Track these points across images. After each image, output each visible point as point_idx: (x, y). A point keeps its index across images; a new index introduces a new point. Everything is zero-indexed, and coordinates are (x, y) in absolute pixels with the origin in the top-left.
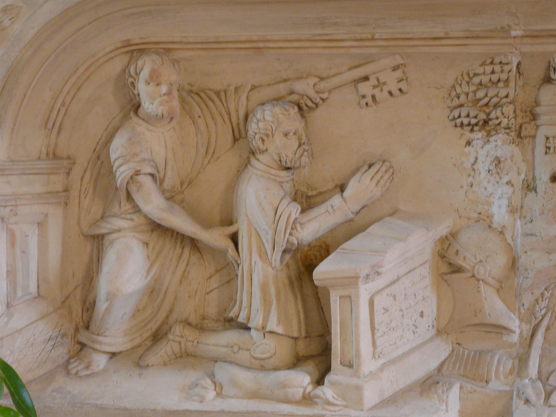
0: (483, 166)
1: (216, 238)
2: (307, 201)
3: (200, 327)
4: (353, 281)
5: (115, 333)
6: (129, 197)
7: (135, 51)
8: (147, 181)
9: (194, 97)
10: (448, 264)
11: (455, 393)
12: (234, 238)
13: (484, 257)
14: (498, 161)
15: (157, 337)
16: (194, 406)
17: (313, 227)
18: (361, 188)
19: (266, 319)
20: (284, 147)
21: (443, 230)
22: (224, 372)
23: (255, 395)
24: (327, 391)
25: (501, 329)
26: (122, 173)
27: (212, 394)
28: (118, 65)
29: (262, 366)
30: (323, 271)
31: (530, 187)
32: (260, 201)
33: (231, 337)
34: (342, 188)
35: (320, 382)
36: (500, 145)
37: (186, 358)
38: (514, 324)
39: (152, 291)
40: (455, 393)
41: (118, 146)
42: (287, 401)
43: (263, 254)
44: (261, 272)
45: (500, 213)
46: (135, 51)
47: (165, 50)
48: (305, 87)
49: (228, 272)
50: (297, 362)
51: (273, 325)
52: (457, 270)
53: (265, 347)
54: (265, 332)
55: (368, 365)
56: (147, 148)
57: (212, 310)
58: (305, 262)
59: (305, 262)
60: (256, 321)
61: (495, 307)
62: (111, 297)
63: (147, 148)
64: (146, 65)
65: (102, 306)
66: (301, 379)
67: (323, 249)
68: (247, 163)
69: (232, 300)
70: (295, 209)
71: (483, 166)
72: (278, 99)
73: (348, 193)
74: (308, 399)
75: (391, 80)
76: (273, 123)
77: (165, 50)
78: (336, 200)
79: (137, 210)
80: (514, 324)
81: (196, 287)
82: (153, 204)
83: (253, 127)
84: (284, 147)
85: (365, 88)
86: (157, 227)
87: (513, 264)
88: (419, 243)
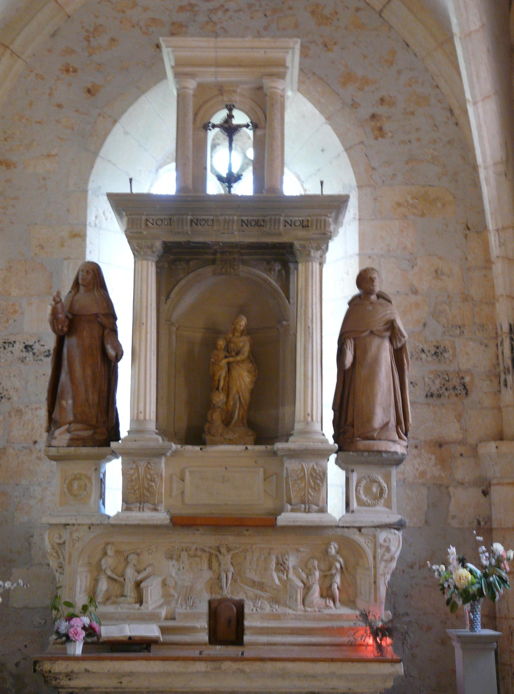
0: (171, 566)
1: (121, 579)
2: (139, 572)
3: (117, 597)
4: (147, 587)
5: (100, 599)
6: (104, 571)
7: (107, 544)
8: (108, 569)
9: (118, 552)
10: (164, 584)
11: (165, 607)
12: (125, 580)
13: (171, 582)
14: (173, 565)
15: (108, 599)
16: (116, 611)
17: (140, 577)
18: (149, 570)
19: (131, 594)
20: (135, 562)
21: (163, 577)
22: (122, 605)
23: (129, 609)
24: (142, 607)
25: (173, 596)
26: (104, 567)
27: (120, 609)
28: (102, 546)
29: (129, 604)
30: (143, 585)
31: (179, 570)
32: (130, 573)
33: (123, 598)
34: (145, 570)
35: (141, 605)
36: (174, 562)
37: (114, 603)
38: (176, 595)
39: (107, 590)
40: (165, 607)
41: (103, 562)
42: (135, 609)
43: (130, 582)
44: (129, 586)
45: (174, 574)
46: (107, 544)
47: (113, 543)
48: (139, 551)
49: (122, 585)
50: (136, 603)
51: (132, 595)
52: (165, 585)
53: (130, 600)
54: (130, 597)
55: (150, 602)
56: (108, 562)
57: (118, 594)
58: (138, 585)
59: (138, 585)
60: (129, 594)
61: (172, 592)
62: (101, 591)
63: (108, 562)
64: (109, 547)
65: (98, 593)
66: (138, 606)
67: (141, 582)
68: (127, 565)
69: (123, 591)
70: (136, 574)
71: (171, 566)
72: (133, 553)
73: (147, 570)
74: (138, 609)
75: (155, 550)
76: (133, 558)
77: (113, 543)
78: (144, 572)
79: (106, 574)
80: (176, 595)
81: (116, 589)
82: (109, 573)
83: (129, 558)
84: (135, 562)
85: (150, 551)
86: (109, 578)
87: (176, 584)
88: (159, 580)
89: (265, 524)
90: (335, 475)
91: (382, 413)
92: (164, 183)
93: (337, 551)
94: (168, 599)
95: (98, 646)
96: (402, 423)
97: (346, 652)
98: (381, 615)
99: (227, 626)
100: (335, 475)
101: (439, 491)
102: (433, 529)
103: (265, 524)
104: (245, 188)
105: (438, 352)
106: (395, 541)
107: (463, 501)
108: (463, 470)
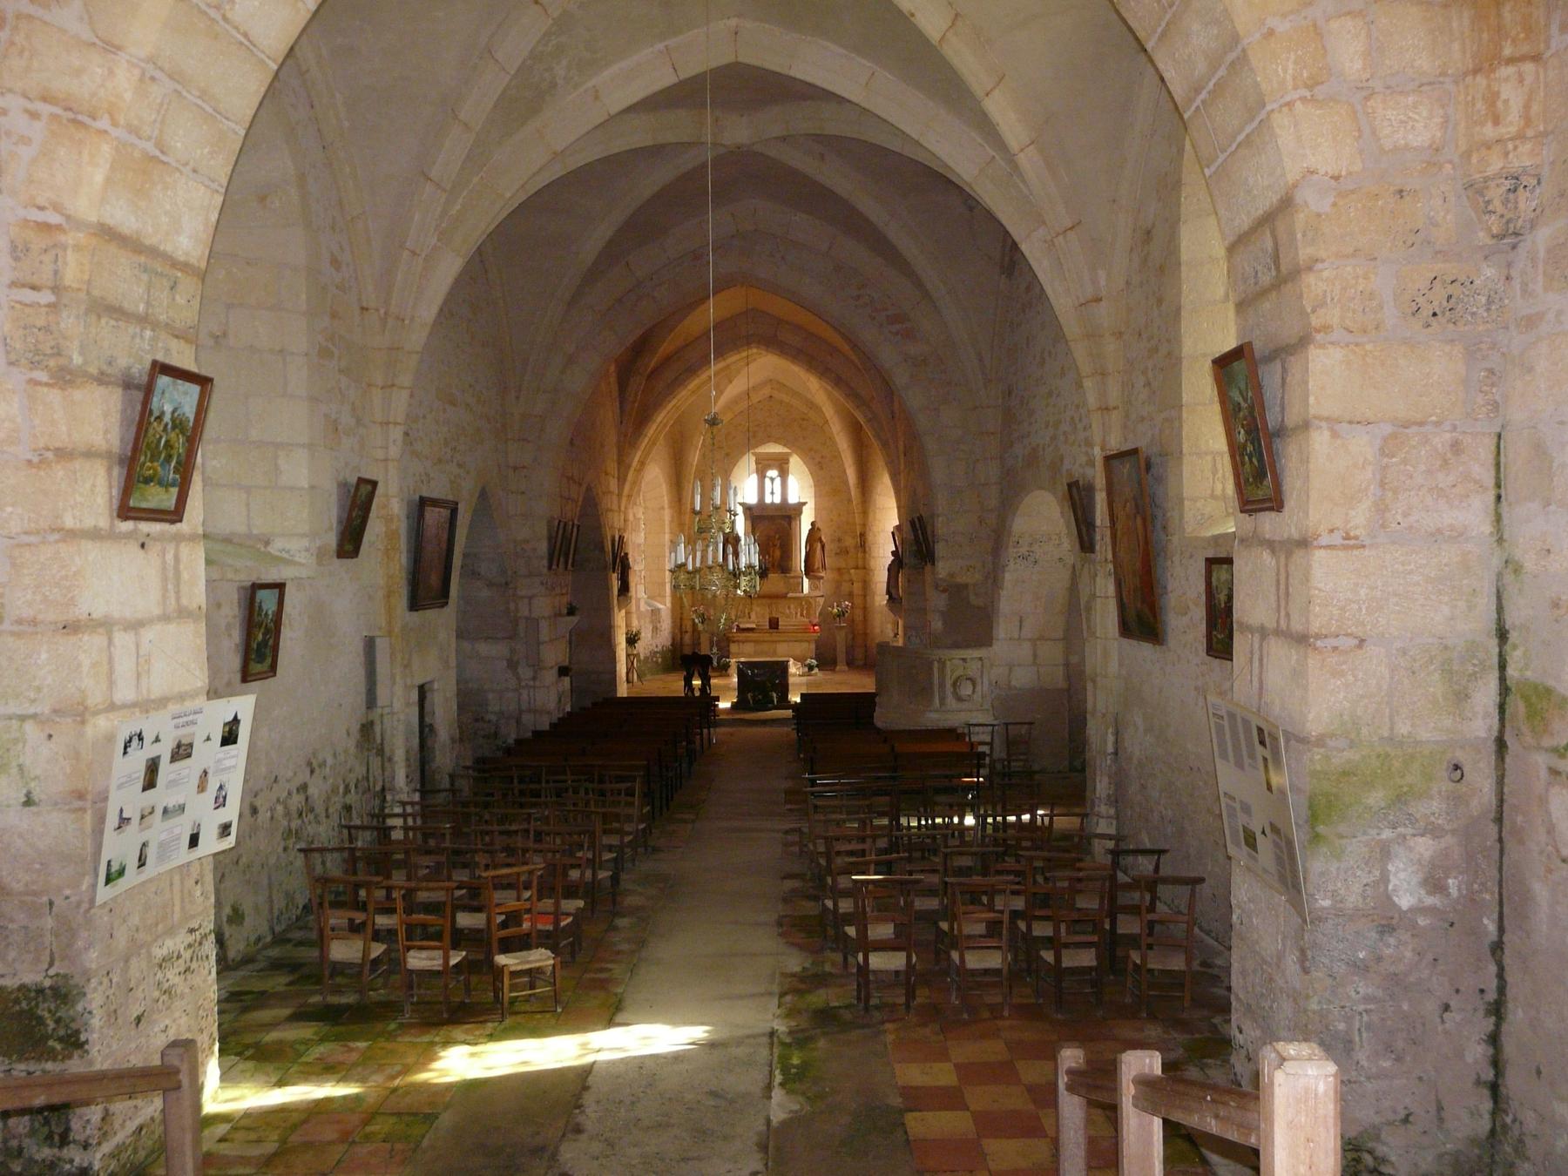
89: (784, 596)
90: (806, 581)
91: (818, 564)
92: (752, 499)
93: (806, 602)
94: (757, 617)
95: (740, 630)
96: (824, 567)
97: (806, 631)
98: (816, 621)
99: (774, 624)
100: (806, 581)
101: (838, 585)
102: (837, 594)
103: (784, 596)
104: (777, 500)
105: (839, 540)
106: (822, 600)
107: (845, 587)
108: (846, 577)
